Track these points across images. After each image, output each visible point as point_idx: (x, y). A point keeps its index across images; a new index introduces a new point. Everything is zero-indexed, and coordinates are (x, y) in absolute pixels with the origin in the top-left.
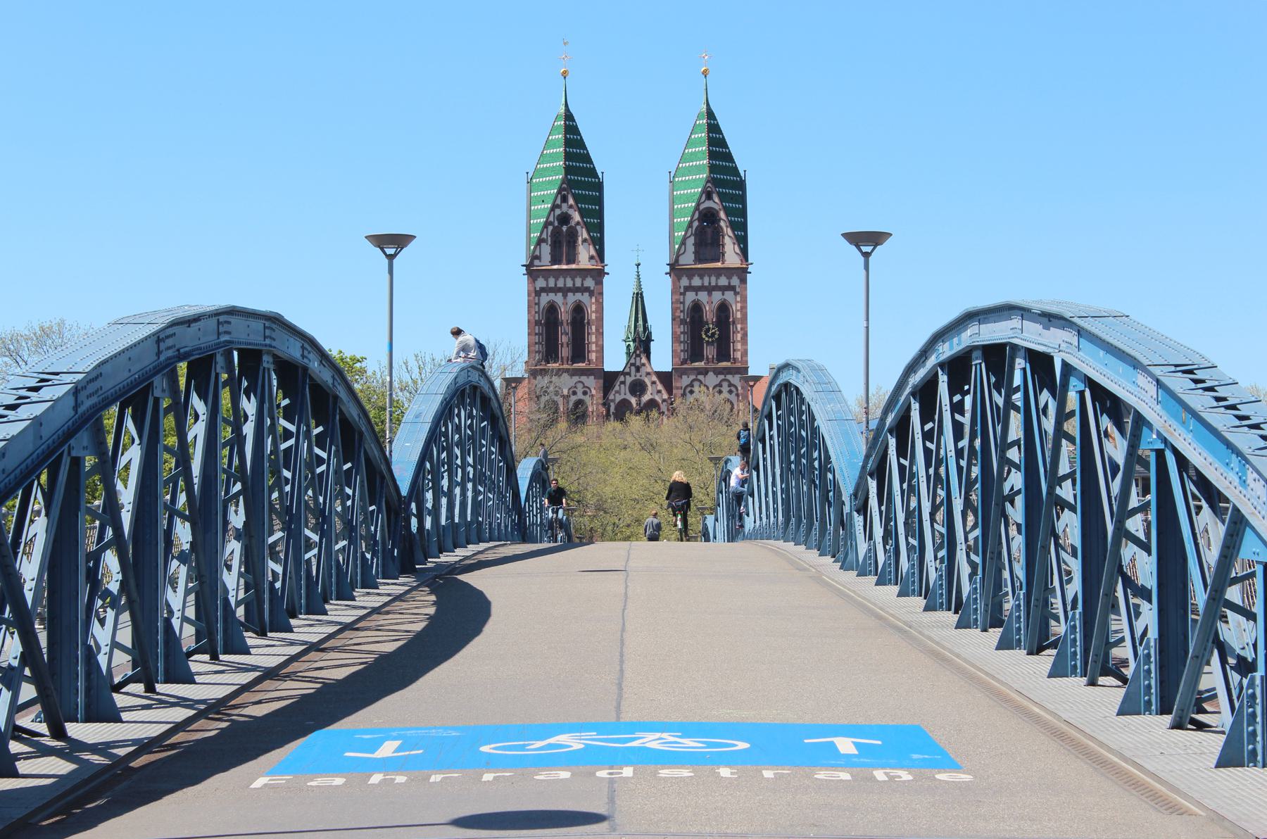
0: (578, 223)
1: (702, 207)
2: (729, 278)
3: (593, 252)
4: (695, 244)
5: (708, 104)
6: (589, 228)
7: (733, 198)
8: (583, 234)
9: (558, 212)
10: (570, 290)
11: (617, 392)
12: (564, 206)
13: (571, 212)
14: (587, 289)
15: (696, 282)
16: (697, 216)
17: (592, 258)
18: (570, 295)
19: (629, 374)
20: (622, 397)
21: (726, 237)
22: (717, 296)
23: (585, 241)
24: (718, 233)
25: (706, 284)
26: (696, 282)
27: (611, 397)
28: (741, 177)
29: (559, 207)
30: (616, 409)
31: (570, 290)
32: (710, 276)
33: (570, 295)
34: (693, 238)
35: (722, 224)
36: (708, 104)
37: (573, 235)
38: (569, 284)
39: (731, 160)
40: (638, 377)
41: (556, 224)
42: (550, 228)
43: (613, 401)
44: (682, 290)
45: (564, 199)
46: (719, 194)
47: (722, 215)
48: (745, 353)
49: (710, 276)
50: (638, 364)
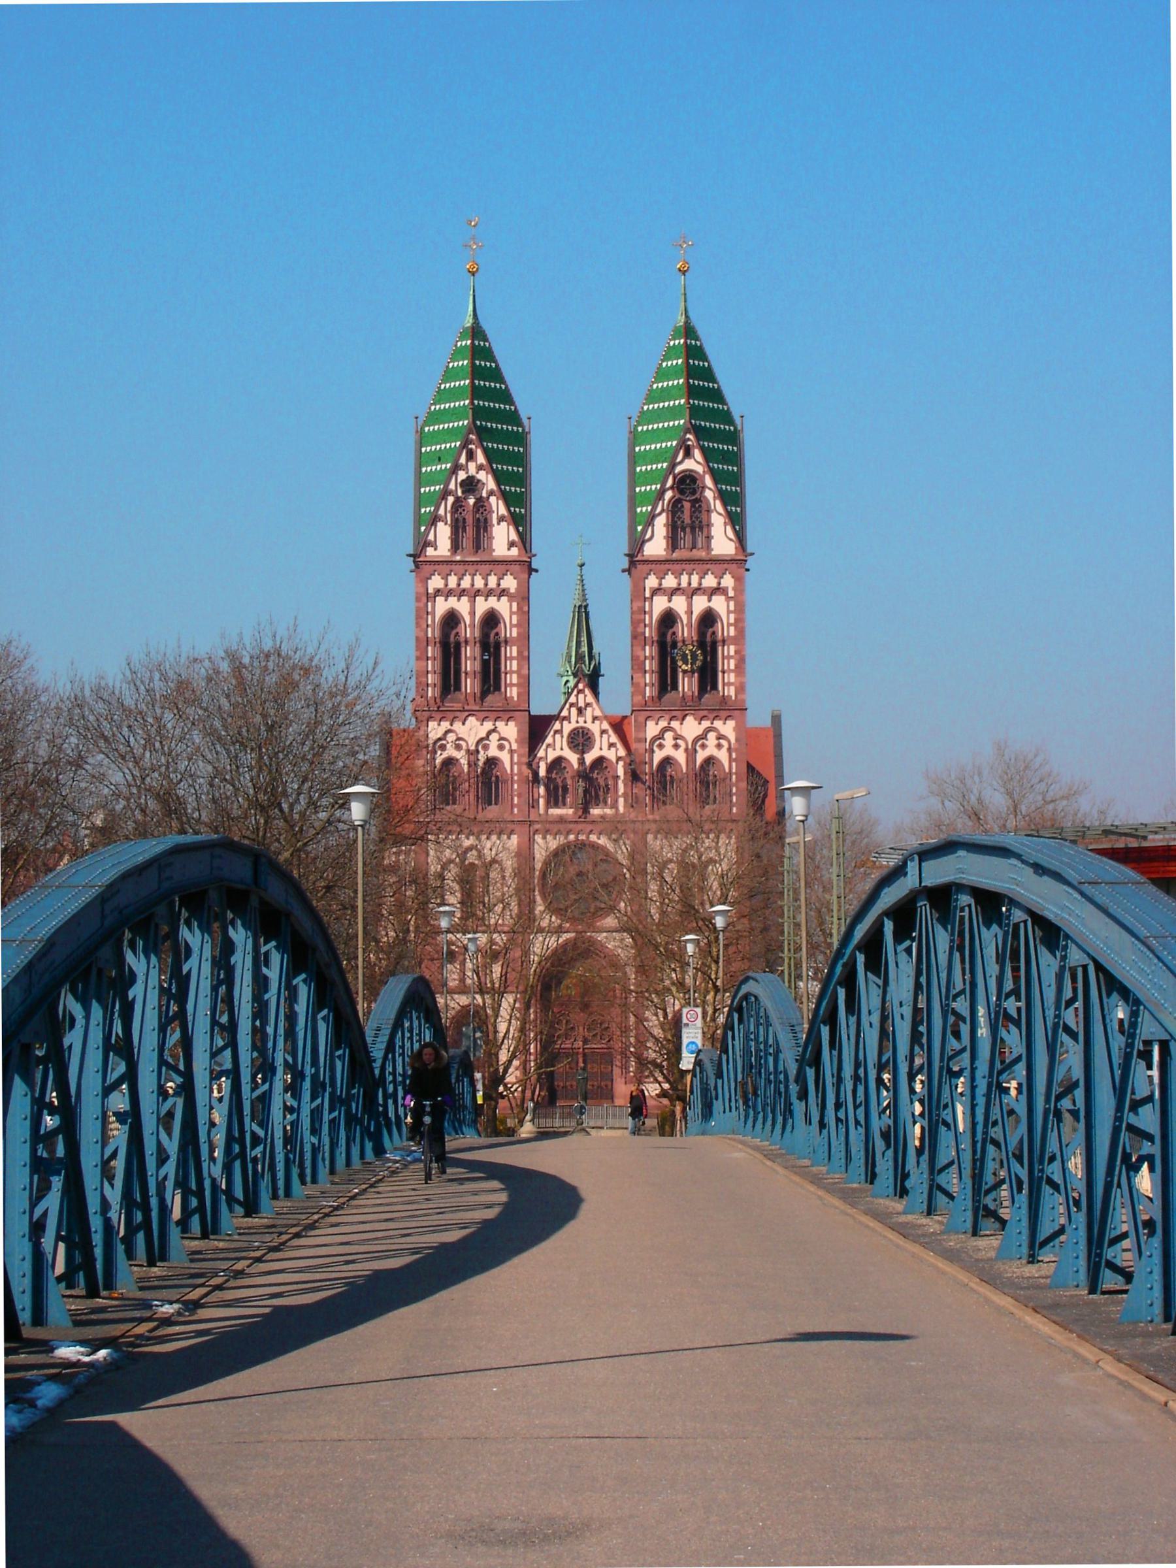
0: (491, 493)
1: (678, 469)
3: (514, 536)
9: (462, 475)
13: (482, 476)
14: (503, 592)
15: (670, 581)
17: (512, 544)
22: (700, 604)
23: (501, 519)
26: (670, 581)
34: (664, 515)
38: (479, 583)
41: (460, 493)
44: (648, 594)
49: (690, 574)
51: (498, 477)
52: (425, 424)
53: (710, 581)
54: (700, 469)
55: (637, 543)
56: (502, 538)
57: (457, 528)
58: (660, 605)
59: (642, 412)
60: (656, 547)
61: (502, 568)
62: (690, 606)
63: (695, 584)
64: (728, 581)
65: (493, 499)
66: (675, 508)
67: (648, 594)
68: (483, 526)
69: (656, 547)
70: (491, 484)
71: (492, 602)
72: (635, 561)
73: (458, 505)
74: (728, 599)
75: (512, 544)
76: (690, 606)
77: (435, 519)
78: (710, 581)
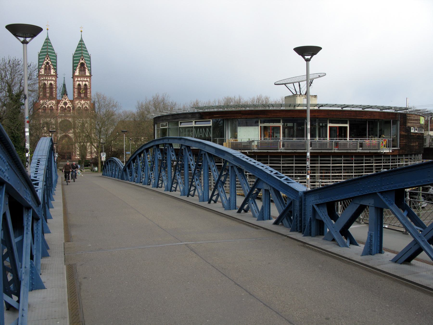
0: (51, 64)
1: (81, 62)
2: (87, 79)
3: (54, 71)
4: (79, 71)
5: (82, 38)
6: (53, 65)
7: (88, 60)
8: (52, 67)
9: (46, 61)
10: (49, 80)
11: (61, 104)
12: (47, 60)
13: (49, 62)
14: (53, 80)
15: (79, 79)
16: (79, 64)
17: (54, 73)
18: (49, 81)
19: (63, 100)
20: (62, 105)
21: (86, 69)
22: (84, 83)
23: (52, 69)
24: (84, 68)
25: (81, 80)
26: (79, 79)
27: (59, 105)
28: (89, 55)
29: (46, 60)
30: (60, 108)
31: (49, 80)
32: (82, 78)
33: (49, 81)
34: (78, 69)
35: (85, 66)
36: (82, 38)
37: (50, 67)
38: (49, 79)
39: (88, 52)
40: (65, 101)
41: (45, 64)
42: (44, 65)
43: (59, 106)
44: (76, 81)
45: (47, 58)
46: (84, 59)
47: (85, 64)
48: (90, 96)
49: (82, 78)
50: (65, 98)
51: (52, 62)
52: (40, 53)
53: (85, 79)
54: (84, 62)
55: (74, 73)
56: (52, 72)
57: (45, 69)
58: (78, 83)
59: (75, 53)
60: (77, 73)
61: (53, 76)
62: (82, 83)
63: (83, 80)
64: (88, 79)
65: (51, 65)
66: (81, 67)
67: (76, 81)
68: (50, 69)
69: (77, 73)
70: (51, 63)
71: (51, 82)
72: (74, 77)
73: (46, 66)
74: (88, 82)
75: (54, 73)
76: (82, 83)
77: (41, 68)
78: (85, 79)
